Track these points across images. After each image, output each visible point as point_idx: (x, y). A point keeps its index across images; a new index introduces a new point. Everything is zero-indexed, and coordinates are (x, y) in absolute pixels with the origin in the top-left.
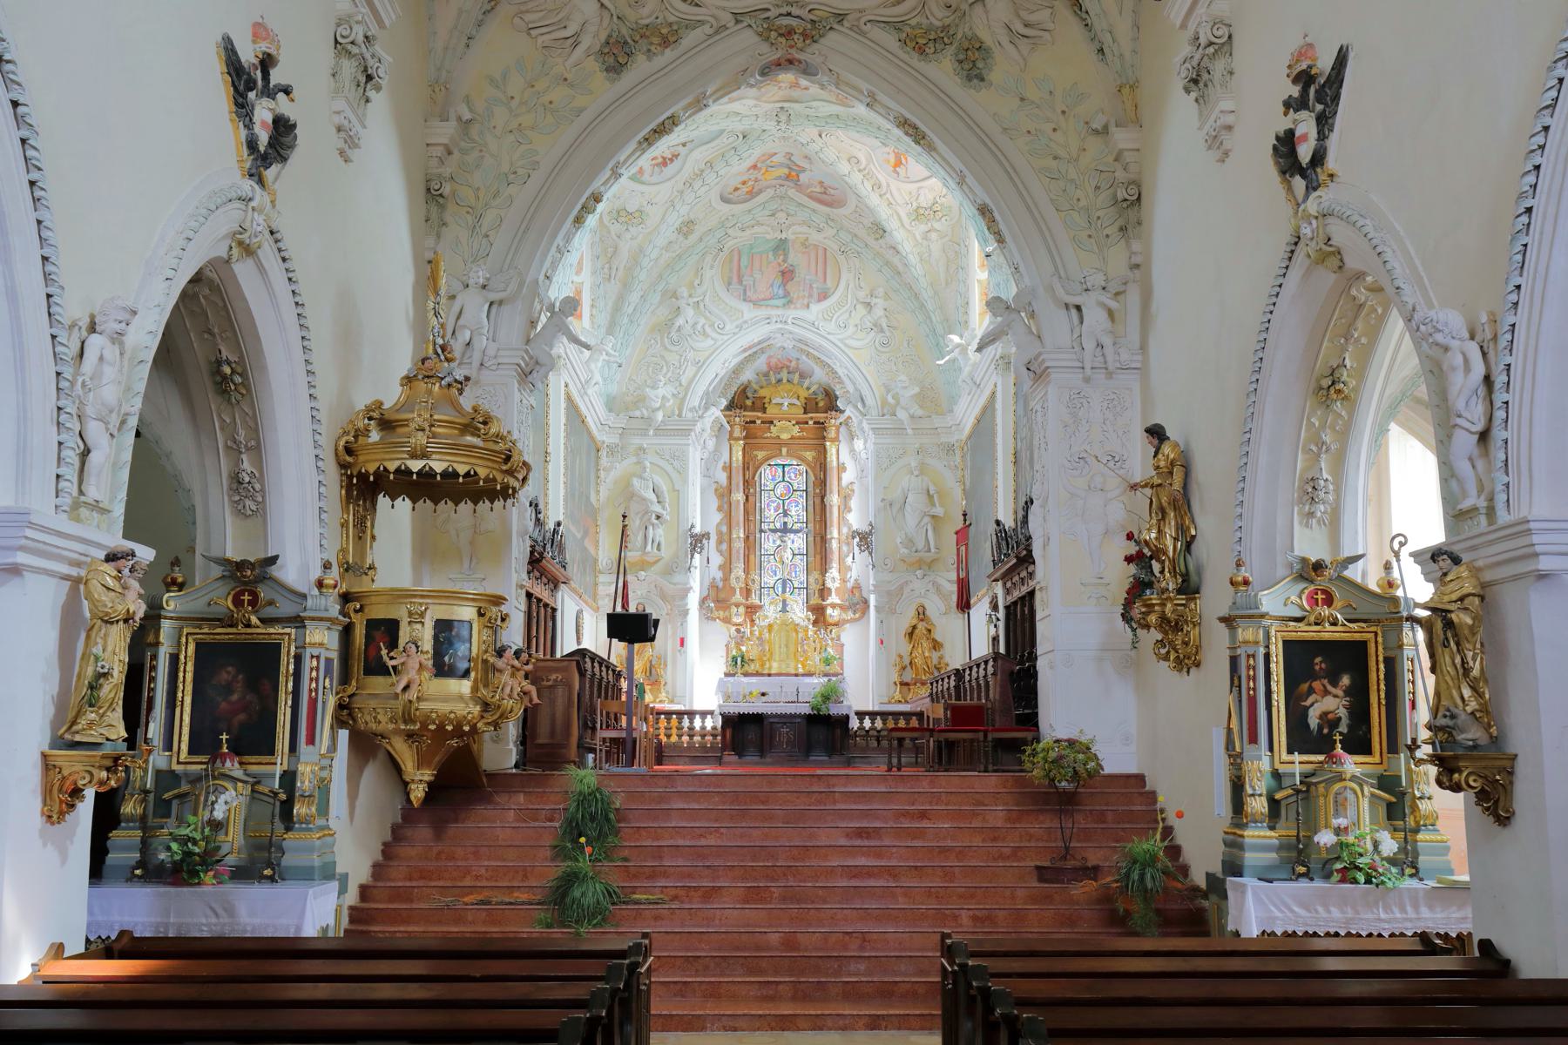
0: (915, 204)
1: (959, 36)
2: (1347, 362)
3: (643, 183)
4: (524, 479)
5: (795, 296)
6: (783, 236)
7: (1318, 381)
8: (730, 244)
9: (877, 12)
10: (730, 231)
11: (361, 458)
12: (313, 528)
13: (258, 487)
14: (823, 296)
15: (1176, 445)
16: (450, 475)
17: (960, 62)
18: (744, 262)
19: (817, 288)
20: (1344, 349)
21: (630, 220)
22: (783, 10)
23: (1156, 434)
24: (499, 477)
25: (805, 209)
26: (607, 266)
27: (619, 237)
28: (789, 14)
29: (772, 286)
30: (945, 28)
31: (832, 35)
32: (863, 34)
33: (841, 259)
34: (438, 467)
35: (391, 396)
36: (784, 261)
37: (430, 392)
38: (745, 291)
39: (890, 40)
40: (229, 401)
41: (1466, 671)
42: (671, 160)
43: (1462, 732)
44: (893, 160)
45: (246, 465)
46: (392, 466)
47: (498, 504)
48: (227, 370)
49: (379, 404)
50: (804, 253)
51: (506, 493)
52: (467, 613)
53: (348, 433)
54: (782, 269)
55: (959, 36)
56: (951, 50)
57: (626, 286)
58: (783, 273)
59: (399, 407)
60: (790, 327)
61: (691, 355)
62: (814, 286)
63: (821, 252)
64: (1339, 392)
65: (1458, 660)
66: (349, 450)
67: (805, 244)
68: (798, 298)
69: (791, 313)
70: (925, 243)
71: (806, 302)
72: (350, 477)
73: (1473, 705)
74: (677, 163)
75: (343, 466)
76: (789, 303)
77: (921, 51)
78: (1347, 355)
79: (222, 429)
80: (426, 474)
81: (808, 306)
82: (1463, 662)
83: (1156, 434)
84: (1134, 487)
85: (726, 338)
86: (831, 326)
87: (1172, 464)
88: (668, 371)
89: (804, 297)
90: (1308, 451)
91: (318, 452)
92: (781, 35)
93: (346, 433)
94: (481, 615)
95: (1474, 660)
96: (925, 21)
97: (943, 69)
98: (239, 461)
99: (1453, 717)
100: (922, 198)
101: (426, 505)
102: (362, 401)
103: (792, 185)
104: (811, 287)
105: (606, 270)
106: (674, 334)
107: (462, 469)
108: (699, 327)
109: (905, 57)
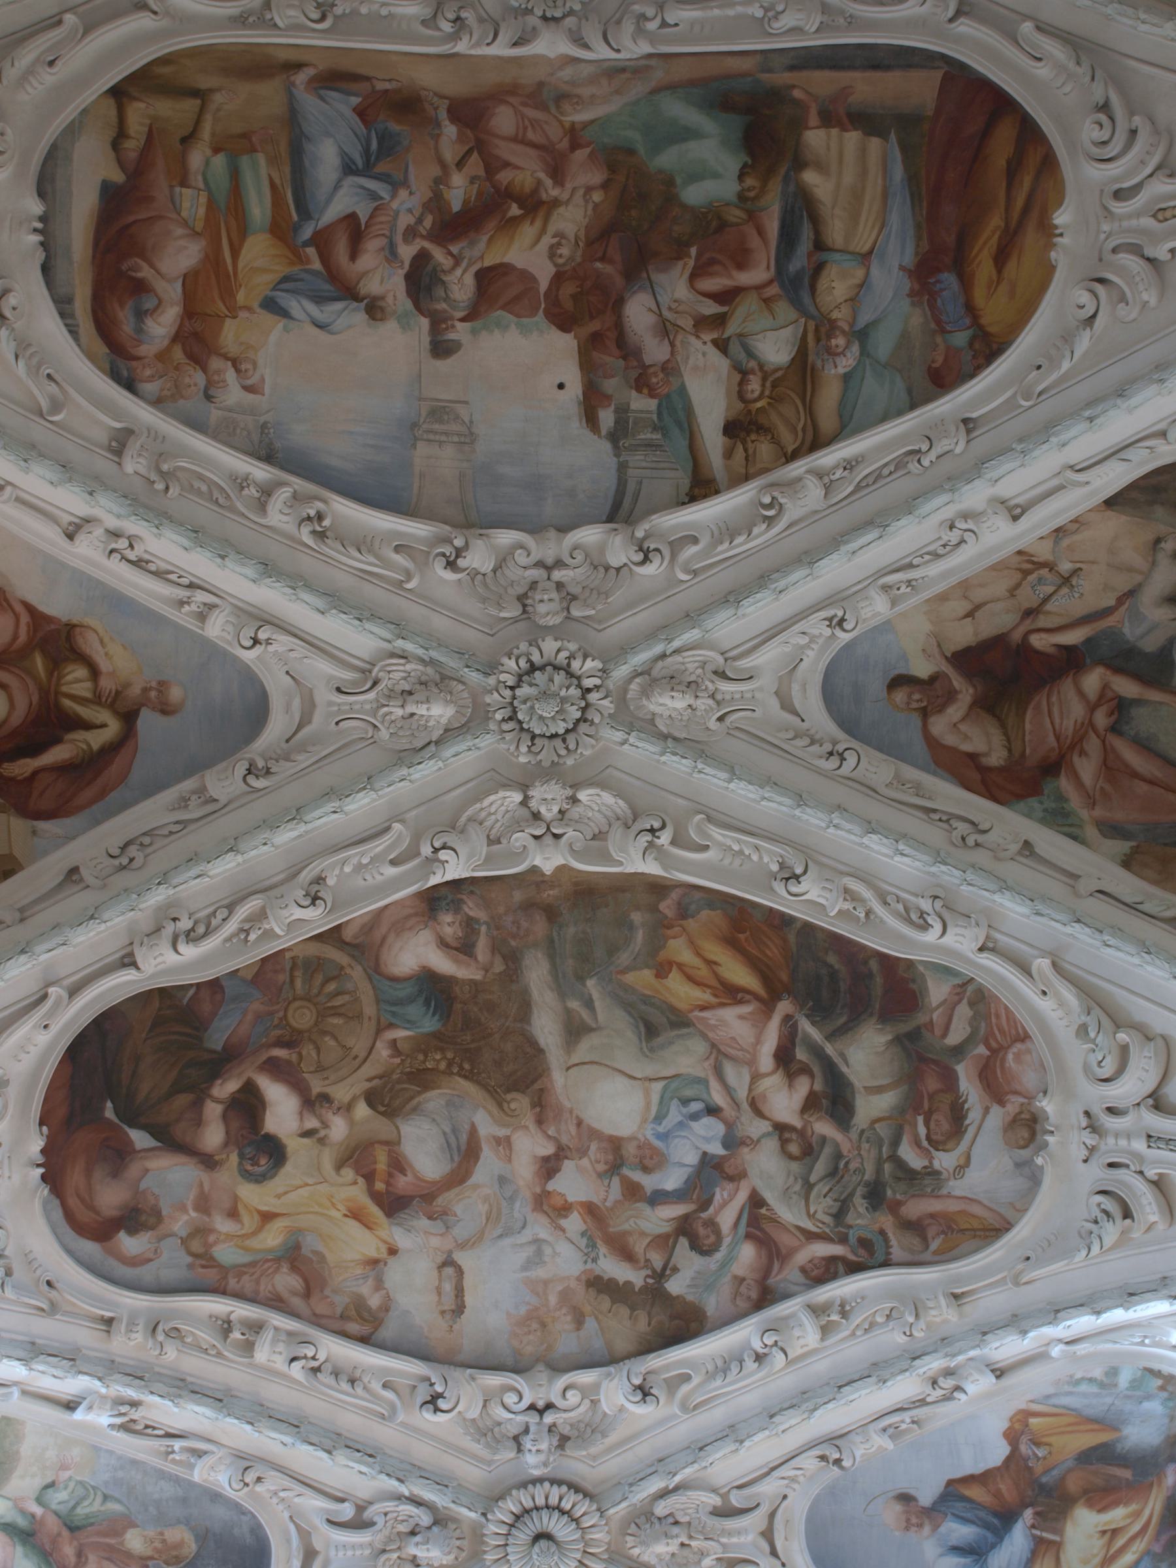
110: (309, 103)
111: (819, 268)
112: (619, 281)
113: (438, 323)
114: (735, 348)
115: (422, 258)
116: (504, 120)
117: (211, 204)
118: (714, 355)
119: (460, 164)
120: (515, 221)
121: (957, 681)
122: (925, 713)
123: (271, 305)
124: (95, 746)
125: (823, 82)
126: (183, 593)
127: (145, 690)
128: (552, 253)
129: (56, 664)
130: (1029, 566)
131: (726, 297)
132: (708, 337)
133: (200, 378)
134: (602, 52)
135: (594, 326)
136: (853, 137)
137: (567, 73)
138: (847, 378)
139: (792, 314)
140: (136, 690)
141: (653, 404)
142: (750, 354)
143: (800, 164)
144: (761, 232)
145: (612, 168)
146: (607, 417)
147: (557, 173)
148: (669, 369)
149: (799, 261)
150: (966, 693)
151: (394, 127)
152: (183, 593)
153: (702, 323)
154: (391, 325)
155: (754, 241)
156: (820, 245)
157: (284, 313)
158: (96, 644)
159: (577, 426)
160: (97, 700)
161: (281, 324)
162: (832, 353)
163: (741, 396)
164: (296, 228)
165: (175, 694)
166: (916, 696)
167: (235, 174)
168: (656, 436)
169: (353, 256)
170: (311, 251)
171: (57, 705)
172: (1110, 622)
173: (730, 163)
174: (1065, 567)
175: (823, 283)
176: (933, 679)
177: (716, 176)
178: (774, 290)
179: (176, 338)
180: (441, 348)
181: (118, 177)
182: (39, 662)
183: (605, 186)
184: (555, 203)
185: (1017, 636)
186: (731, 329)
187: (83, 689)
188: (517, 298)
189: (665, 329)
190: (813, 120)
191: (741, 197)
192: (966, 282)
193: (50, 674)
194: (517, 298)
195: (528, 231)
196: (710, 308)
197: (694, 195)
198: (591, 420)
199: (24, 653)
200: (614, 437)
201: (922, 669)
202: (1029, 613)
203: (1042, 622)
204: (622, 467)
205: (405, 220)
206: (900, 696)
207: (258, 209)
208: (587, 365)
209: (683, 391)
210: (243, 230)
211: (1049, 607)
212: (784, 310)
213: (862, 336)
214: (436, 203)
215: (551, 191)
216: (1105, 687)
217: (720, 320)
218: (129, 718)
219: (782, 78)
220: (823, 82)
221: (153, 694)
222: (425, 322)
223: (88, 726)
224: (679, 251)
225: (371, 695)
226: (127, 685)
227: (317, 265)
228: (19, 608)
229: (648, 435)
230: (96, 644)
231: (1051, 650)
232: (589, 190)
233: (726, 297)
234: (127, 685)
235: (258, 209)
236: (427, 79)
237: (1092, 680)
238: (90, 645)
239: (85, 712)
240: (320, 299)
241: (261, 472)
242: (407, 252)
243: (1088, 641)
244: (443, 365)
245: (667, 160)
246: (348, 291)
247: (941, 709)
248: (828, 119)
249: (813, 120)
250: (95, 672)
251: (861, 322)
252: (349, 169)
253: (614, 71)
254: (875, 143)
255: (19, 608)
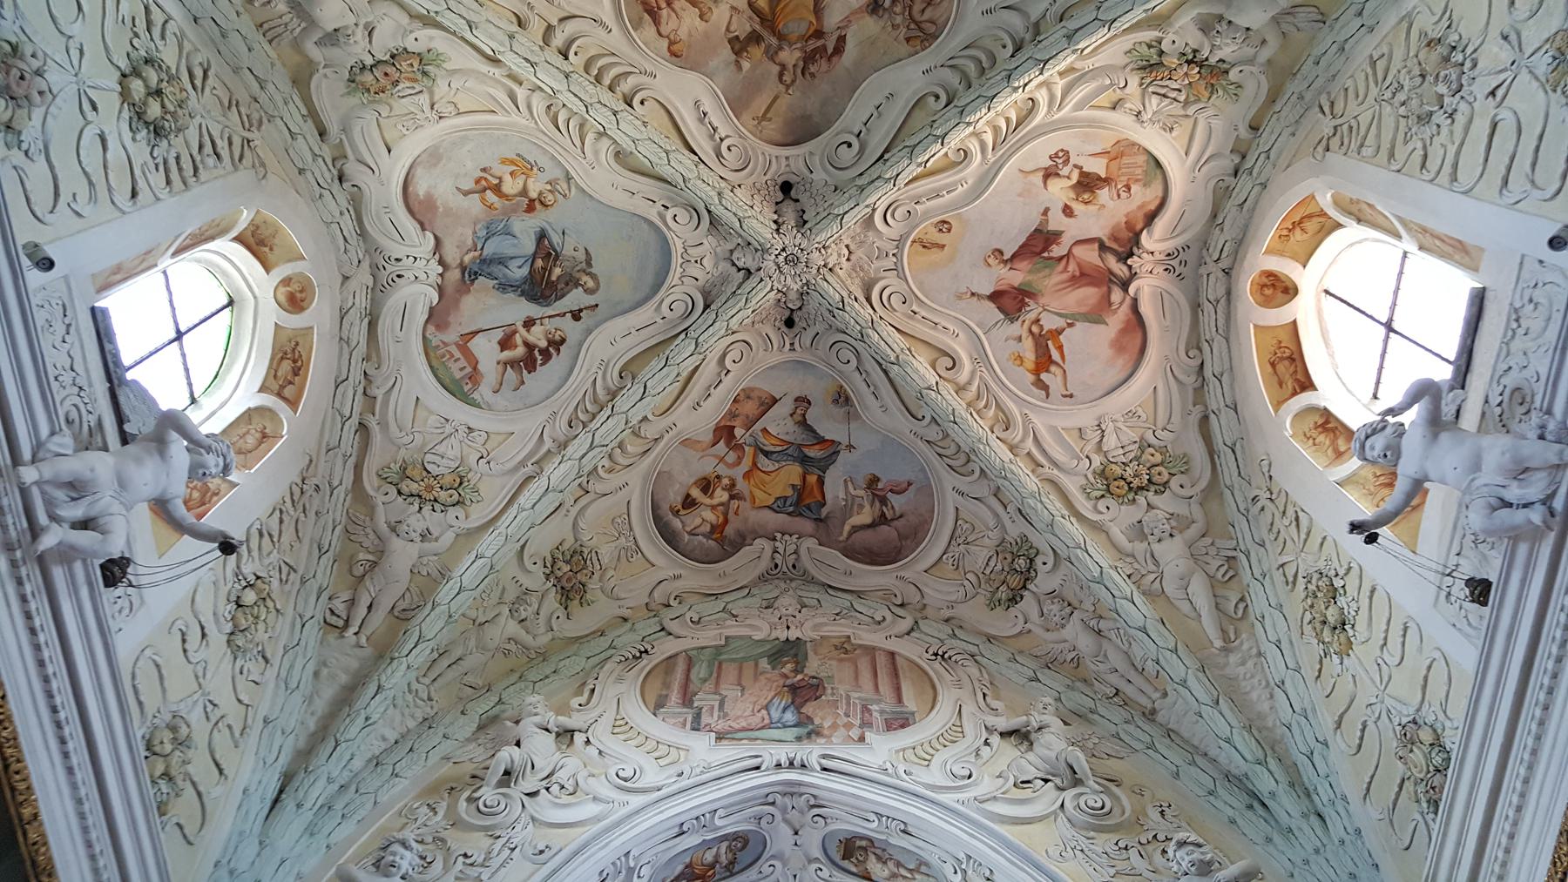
0: (1097, 460)
3: (474, 404)
5: (827, 724)
6: (794, 634)
8: (667, 647)
10: (673, 626)
14: (899, 722)
18: (700, 671)
19: (882, 712)
21: (430, 488)
25: (839, 594)
26: (346, 596)
27: (393, 530)
29: (767, 707)
33: (935, 669)
36: (796, 671)
38: (697, 717)
42: (546, 355)
44: (1030, 356)
50: (841, 660)
54: (789, 682)
57: (383, 653)
58: (794, 689)
60: (816, 779)
61: (524, 834)
62: (874, 707)
63: (882, 661)
67: (845, 648)
68: (834, 727)
69: (812, 752)
70: (1140, 547)
71: (855, 733)
74: (558, 363)
76: (812, 732)
81: (862, 739)
85: (637, 801)
86: (935, 776)
88: (446, 869)
89: (849, 726)
100: (1111, 442)
103: (807, 525)
104: (865, 709)
105: (340, 607)
106: (488, 794)
108: (561, 776)
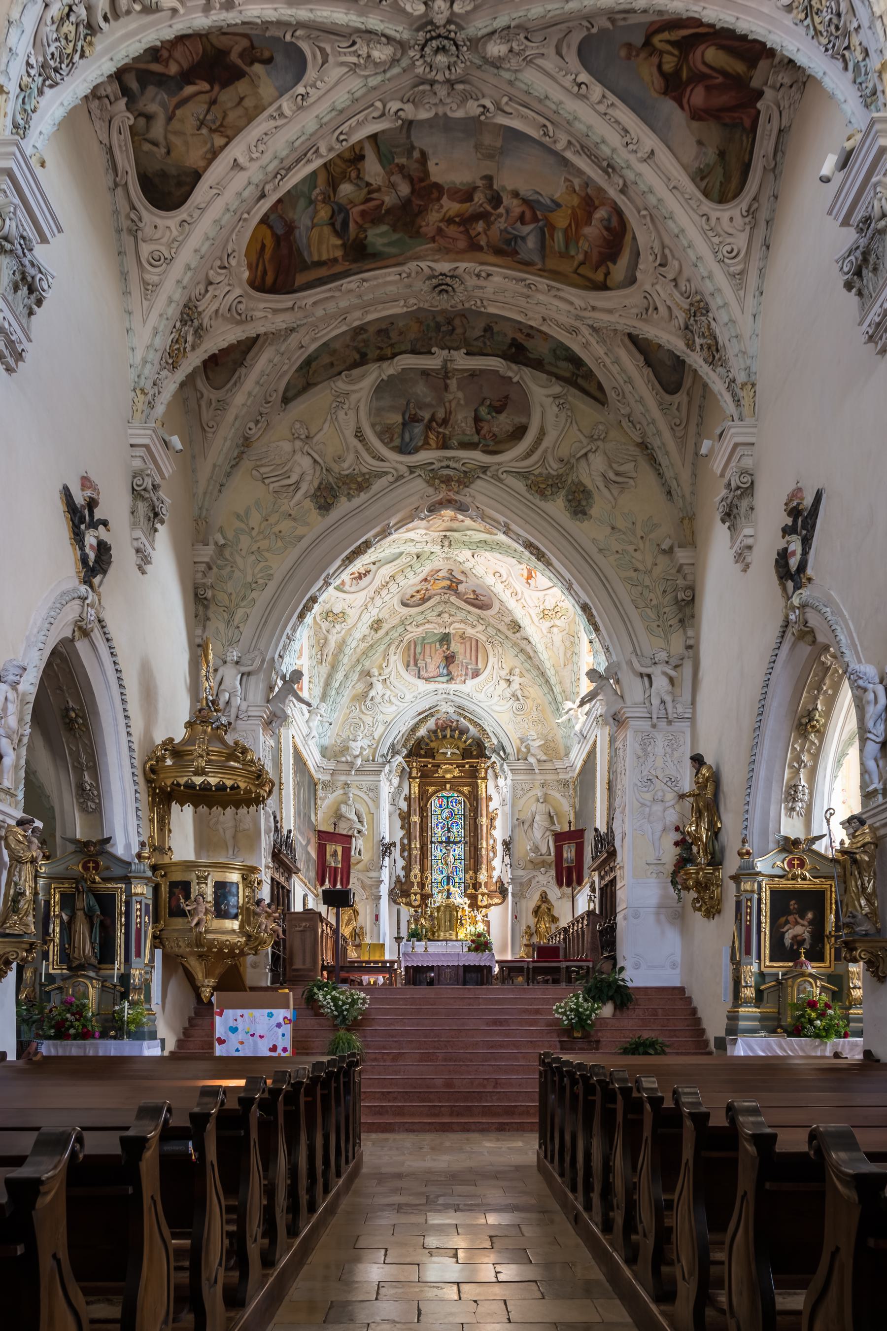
1: (569, 481)
2: (819, 707)
4: (270, 792)
7: (799, 720)
9: (511, 464)
11: (162, 776)
12: (133, 822)
13: (95, 793)
15: (710, 767)
16: (221, 788)
17: (570, 501)
20: (816, 698)
22: (444, 464)
23: (698, 760)
24: (253, 789)
28: (448, 467)
30: (560, 476)
31: (479, 482)
32: (501, 481)
34: (213, 781)
35: (179, 734)
37: (205, 732)
39: (519, 485)
40: (74, 736)
41: (864, 889)
43: (859, 925)
45: (87, 778)
46: (183, 781)
47: (253, 809)
48: (73, 715)
49: (171, 740)
51: (258, 801)
52: (234, 877)
53: (150, 759)
55: (569, 481)
56: (563, 493)
59: (184, 742)
64: (814, 727)
65: (859, 882)
66: (153, 770)
72: (154, 789)
73: (867, 909)
75: (149, 781)
77: (542, 494)
78: (819, 702)
79: (70, 754)
80: (206, 787)
82: (863, 884)
83: (698, 760)
84: (682, 797)
87: (707, 780)
90: (791, 767)
91: (134, 770)
92: (442, 482)
93: (150, 759)
94: (244, 879)
95: (869, 882)
96: (545, 472)
97: (557, 507)
98: (82, 776)
99: (854, 917)
101: (203, 809)
102: (159, 739)
107: (229, 783)
109: (530, 497)
110: (536, 259)
111: (332, 217)
112: (413, 199)
113: (490, 186)
114: (363, 185)
115: (496, 207)
116: (462, 244)
117: (577, 243)
118: (372, 181)
119: (479, 234)
120: (457, 216)
121: (239, 62)
122: (253, 47)
123: (558, 205)
124: (666, 33)
125: (338, 269)
126: (610, 111)
127: (637, 55)
128: (442, 207)
129: (677, 72)
130: (222, 129)
131: (367, 200)
132: (375, 186)
133: (589, 191)
134: (423, 265)
135: (423, 184)
136: (324, 257)
137: (437, 257)
138: (315, 187)
139: (341, 201)
140: (643, 55)
141: (396, 161)
142: (357, 185)
143: (344, 245)
144: (356, 223)
145: (418, 232)
146: (416, 154)
147: (440, 231)
148: (390, 173)
149: (339, 219)
150: (234, 57)
151: (505, 247)
152: (610, 111)
153: (378, 190)
154: (509, 188)
155: (359, 220)
156: (333, 225)
157: (553, 201)
158: (656, 82)
159: (429, 151)
160: (661, 53)
161: (556, 196)
162: (323, 193)
163: (359, 170)
164: (545, 225)
165: (623, 53)
166: (258, 54)
167: (567, 247)
168: (394, 150)
169: (523, 213)
170: (540, 217)
171: (681, 53)
172: (175, 100)
173: (370, 239)
174: (204, 131)
175: (330, 214)
176: (251, 63)
177: (376, 235)
178: (349, 207)
179: (596, 208)
180: (489, 179)
181: (610, 264)
182: (684, 75)
183: (420, 227)
184: (441, 221)
185: (217, 88)
186: (365, 190)
187: (667, 58)
188: (456, 193)
189: (393, 186)
190: (340, 259)
191: (365, 231)
192: (274, 234)
193: (681, 67)
194: (456, 193)
195: (451, 213)
196: (374, 195)
197: (384, 228)
198: (423, 154)
199: (690, 81)
200: (413, 148)
201: (258, 68)
202: (213, 102)
203: (206, 97)
204: (409, 136)
205: (502, 220)
206: (267, 54)
207: (559, 236)
208: (426, 173)
209: (384, 168)
210: (566, 231)
211: (205, 106)
212: (344, 201)
213: (311, 202)
214: (489, 224)
215: (443, 225)
216: (167, 66)
217: (369, 193)
218: (647, 43)
219: (354, 266)
220: (338, 269)
221: (634, 53)
222: (495, 187)
223: (668, 42)
224: (388, 211)
225: (527, 53)
226: (646, 59)
227: (538, 213)
228: (686, 106)
229: (398, 150)
230: (656, 82)
231: (198, 81)
232: (427, 225)
233: (367, 200)
234: (646, 59)
235: (559, 236)
236: (492, 259)
237: (173, 69)
238: (658, 82)
239: (669, 48)
240: (538, 202)
241: (569, 155)
242: (501, 210)
243: (181, 88)
244: (488, 172)
245: (395, 236)
246: (525, 201)
247: (245, 50)
248: (335, 260)
249: (340, 259)
250: (660, 67)
251: (312, 206)
252: (523, 239)
253: (418, 258)
254: (316, 258)
255: (686, 106)
